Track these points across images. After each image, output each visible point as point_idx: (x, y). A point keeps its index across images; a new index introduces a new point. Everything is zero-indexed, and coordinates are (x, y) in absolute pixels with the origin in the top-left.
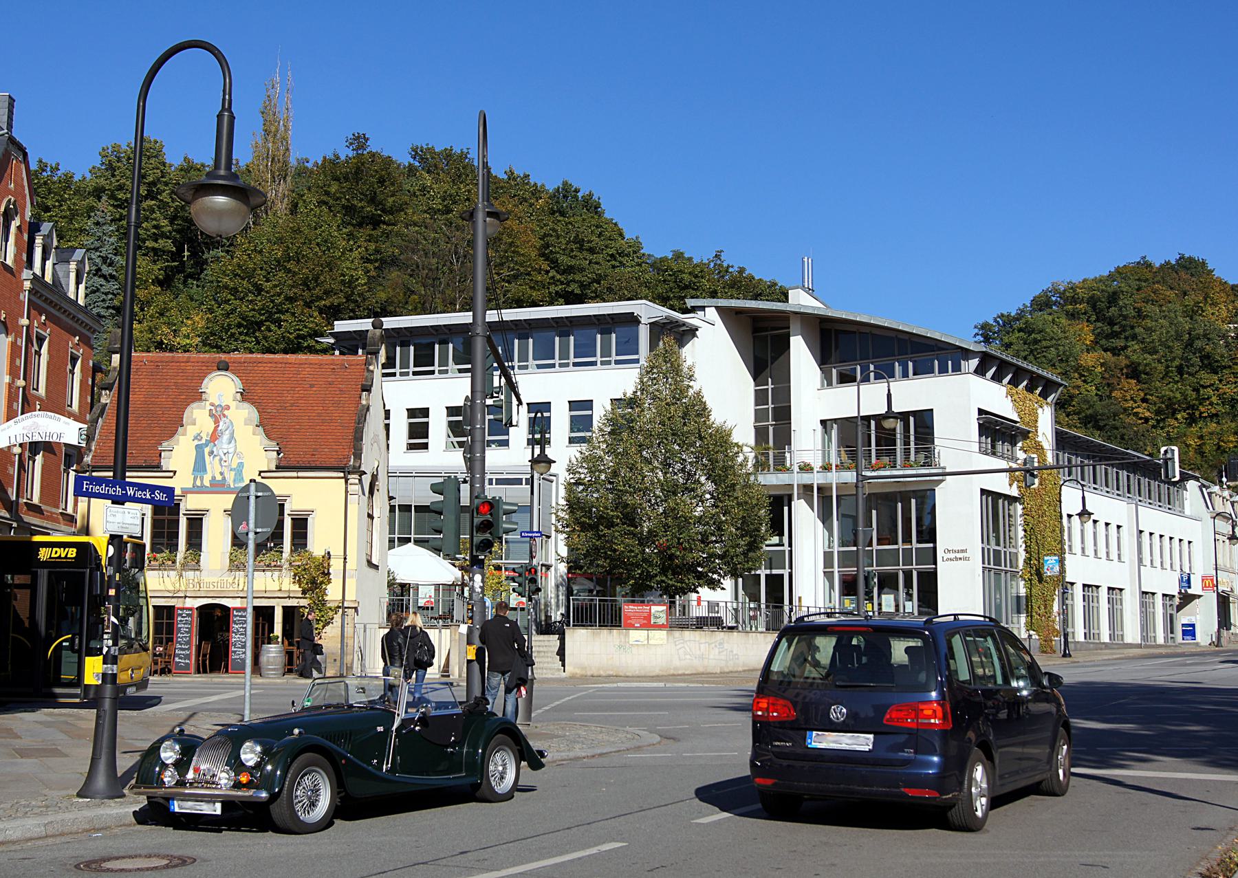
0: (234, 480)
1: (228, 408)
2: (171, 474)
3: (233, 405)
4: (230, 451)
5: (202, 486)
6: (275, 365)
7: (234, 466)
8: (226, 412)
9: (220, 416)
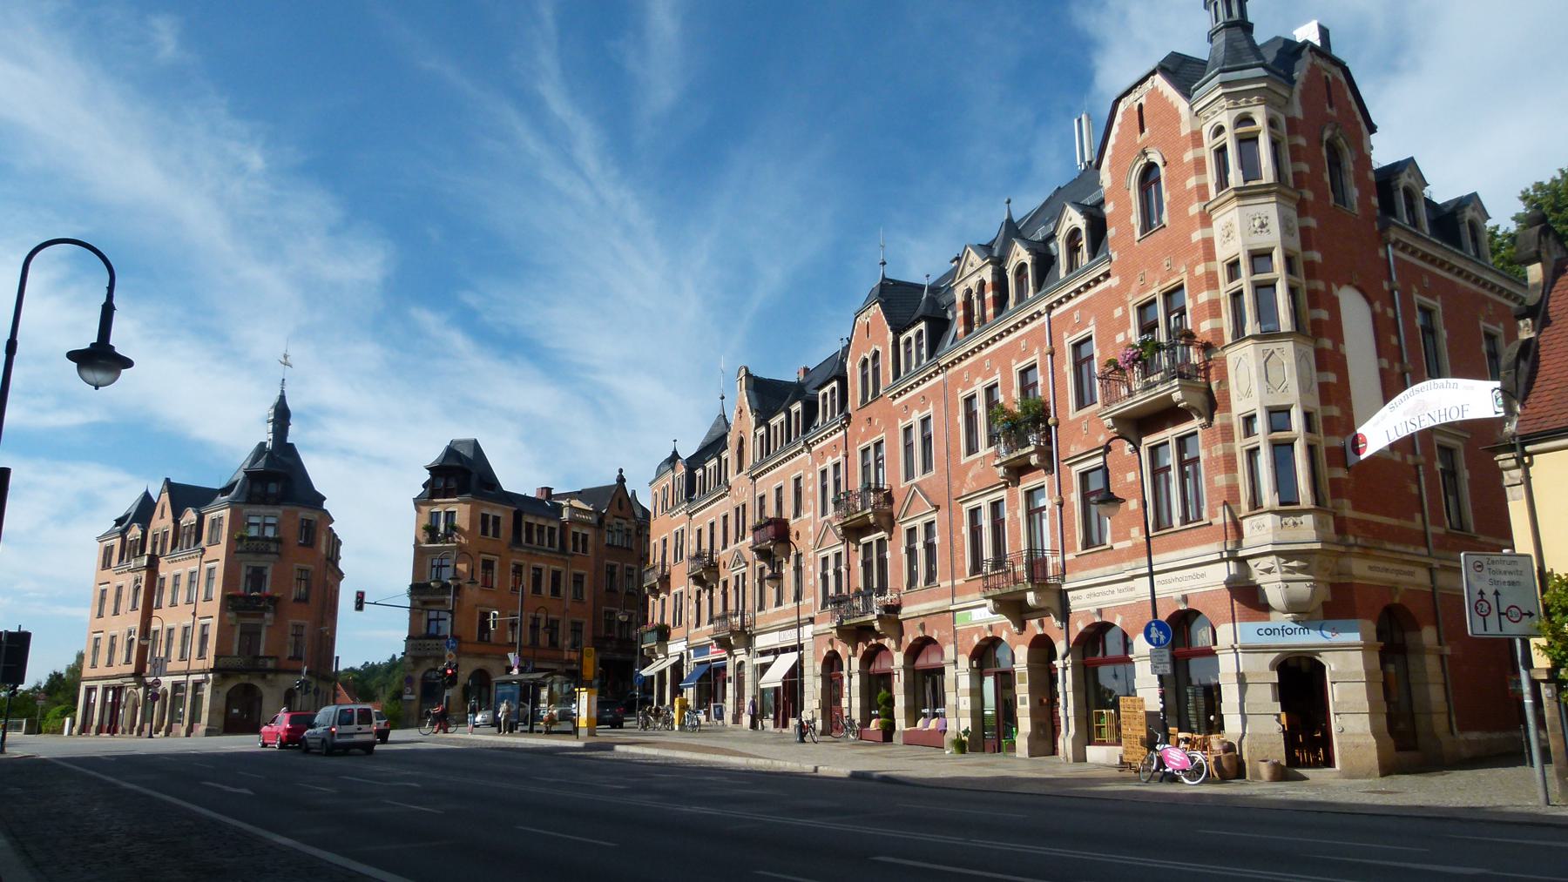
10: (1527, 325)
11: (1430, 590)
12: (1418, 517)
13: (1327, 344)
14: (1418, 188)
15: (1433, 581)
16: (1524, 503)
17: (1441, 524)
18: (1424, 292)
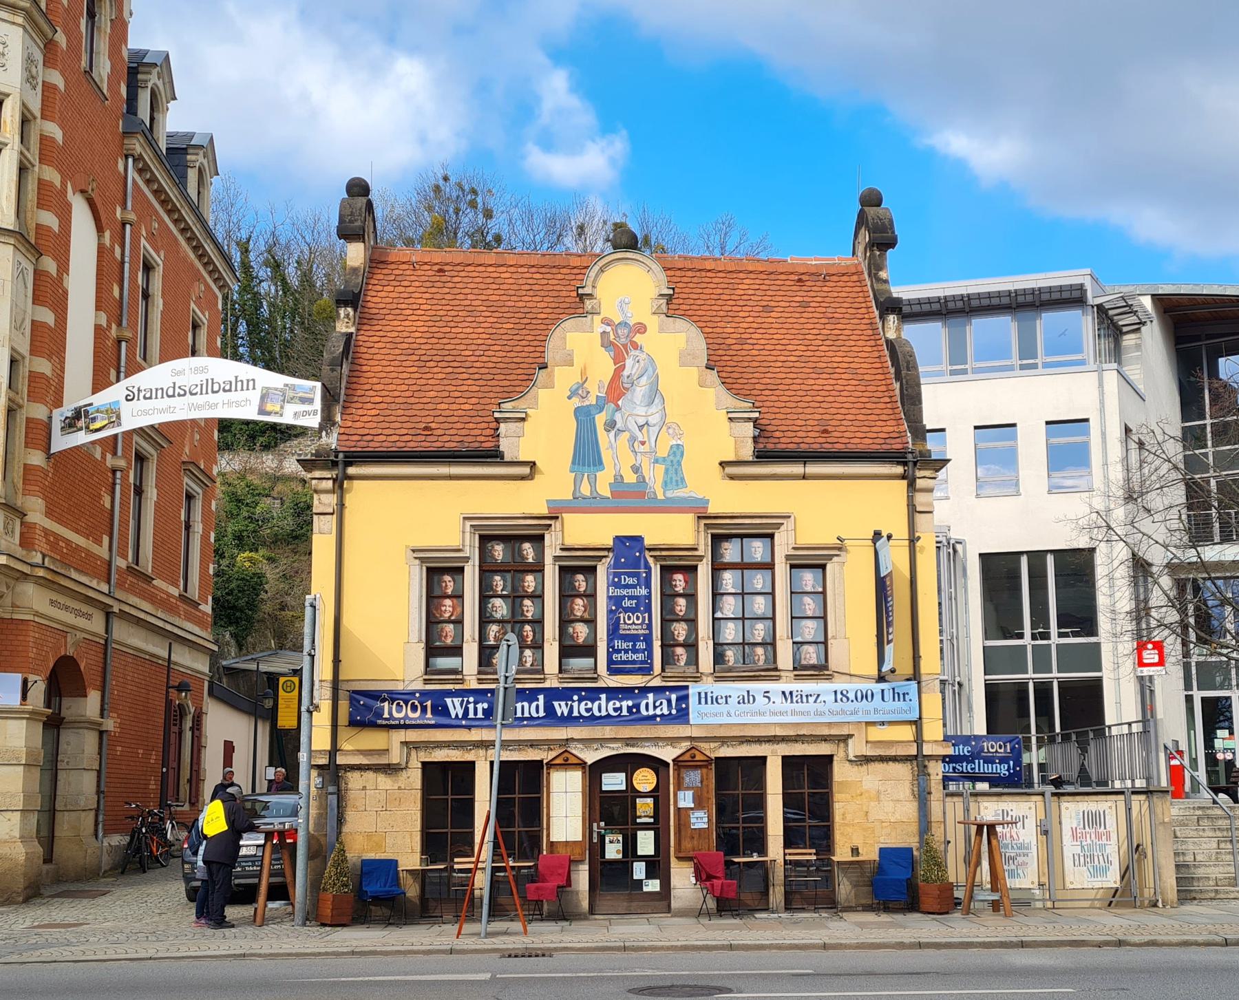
0: (665, 484)
1: (641, 328)
2: (526, 470)
3: (653, 322)
4: (652, 420)
5: (595, 496)
6: (678, 273)
7: (663, 452)
8: (638, 338)
9: (625, 346)
10: (347, 316)
11: (102, 642)
12: (106, 539)
13: (50, 265)
14: (164, 99)
15: (108, 630)
16: (332, 539)
17: (125, 557)
18: (151, 237)
